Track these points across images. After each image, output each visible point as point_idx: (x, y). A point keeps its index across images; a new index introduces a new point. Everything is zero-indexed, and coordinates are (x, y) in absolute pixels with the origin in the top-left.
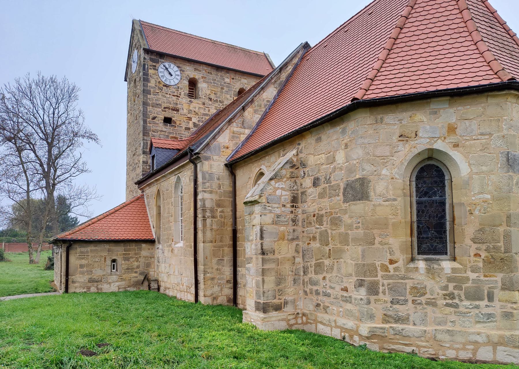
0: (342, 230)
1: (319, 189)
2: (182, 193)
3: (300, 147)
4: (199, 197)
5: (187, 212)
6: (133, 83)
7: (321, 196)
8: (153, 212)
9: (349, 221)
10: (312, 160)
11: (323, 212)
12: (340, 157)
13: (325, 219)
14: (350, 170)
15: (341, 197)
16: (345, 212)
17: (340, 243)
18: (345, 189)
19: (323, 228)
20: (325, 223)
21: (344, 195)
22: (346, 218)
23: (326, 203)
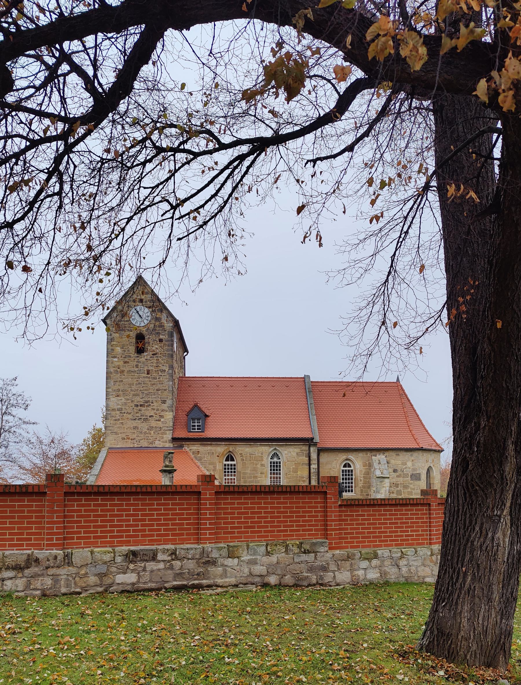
0: (409, 490)
1: (397, 474)
2: (271, 459)
3: (385, 454)
4: (311, 467)
5: (291, 473)
6: (133, 334)
7: (398, 476)
8: (215, 467)
9: (413, 487)
10: (392, 462)
11: (399, 483)
12: (409, 464)
13: (400, 485)
14: (414, 470)
15: (409, 478)
16: (411, 484)
17: (408, 494)
18: (411, 476)
19: (398, 489)
20: (399, 487)
21: (411, 478)
22: (411, 486)
23: (401, 480)
